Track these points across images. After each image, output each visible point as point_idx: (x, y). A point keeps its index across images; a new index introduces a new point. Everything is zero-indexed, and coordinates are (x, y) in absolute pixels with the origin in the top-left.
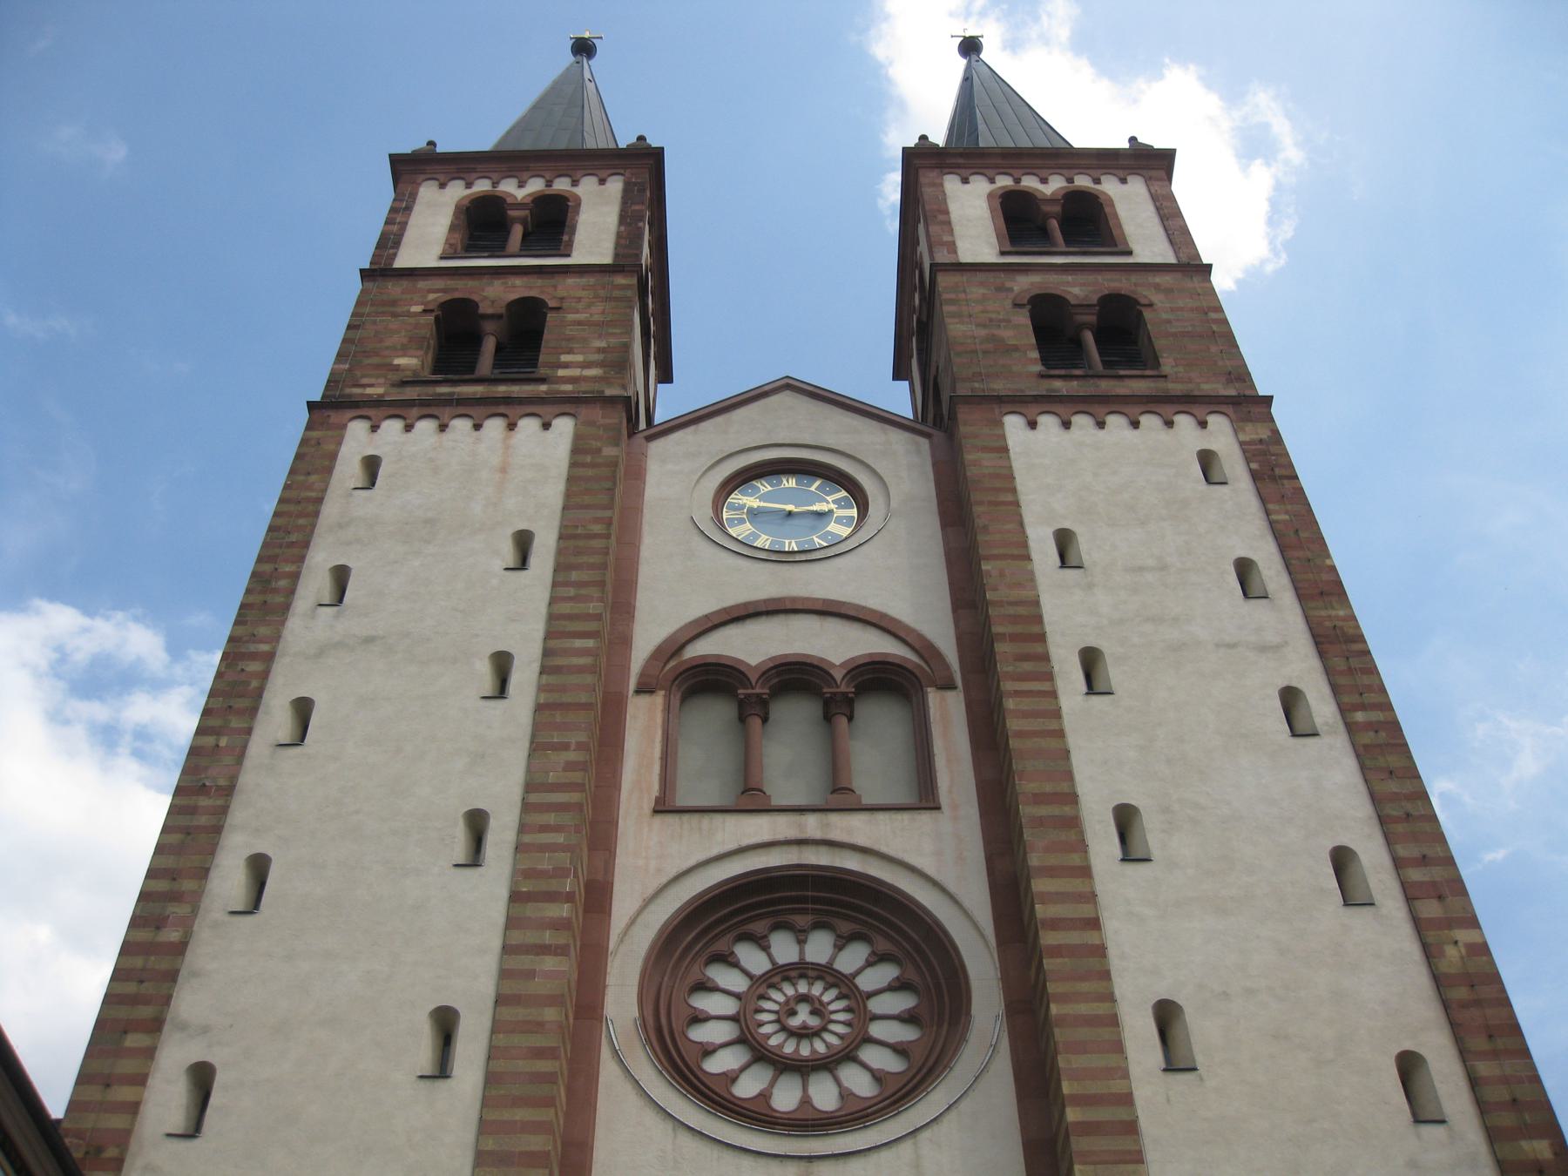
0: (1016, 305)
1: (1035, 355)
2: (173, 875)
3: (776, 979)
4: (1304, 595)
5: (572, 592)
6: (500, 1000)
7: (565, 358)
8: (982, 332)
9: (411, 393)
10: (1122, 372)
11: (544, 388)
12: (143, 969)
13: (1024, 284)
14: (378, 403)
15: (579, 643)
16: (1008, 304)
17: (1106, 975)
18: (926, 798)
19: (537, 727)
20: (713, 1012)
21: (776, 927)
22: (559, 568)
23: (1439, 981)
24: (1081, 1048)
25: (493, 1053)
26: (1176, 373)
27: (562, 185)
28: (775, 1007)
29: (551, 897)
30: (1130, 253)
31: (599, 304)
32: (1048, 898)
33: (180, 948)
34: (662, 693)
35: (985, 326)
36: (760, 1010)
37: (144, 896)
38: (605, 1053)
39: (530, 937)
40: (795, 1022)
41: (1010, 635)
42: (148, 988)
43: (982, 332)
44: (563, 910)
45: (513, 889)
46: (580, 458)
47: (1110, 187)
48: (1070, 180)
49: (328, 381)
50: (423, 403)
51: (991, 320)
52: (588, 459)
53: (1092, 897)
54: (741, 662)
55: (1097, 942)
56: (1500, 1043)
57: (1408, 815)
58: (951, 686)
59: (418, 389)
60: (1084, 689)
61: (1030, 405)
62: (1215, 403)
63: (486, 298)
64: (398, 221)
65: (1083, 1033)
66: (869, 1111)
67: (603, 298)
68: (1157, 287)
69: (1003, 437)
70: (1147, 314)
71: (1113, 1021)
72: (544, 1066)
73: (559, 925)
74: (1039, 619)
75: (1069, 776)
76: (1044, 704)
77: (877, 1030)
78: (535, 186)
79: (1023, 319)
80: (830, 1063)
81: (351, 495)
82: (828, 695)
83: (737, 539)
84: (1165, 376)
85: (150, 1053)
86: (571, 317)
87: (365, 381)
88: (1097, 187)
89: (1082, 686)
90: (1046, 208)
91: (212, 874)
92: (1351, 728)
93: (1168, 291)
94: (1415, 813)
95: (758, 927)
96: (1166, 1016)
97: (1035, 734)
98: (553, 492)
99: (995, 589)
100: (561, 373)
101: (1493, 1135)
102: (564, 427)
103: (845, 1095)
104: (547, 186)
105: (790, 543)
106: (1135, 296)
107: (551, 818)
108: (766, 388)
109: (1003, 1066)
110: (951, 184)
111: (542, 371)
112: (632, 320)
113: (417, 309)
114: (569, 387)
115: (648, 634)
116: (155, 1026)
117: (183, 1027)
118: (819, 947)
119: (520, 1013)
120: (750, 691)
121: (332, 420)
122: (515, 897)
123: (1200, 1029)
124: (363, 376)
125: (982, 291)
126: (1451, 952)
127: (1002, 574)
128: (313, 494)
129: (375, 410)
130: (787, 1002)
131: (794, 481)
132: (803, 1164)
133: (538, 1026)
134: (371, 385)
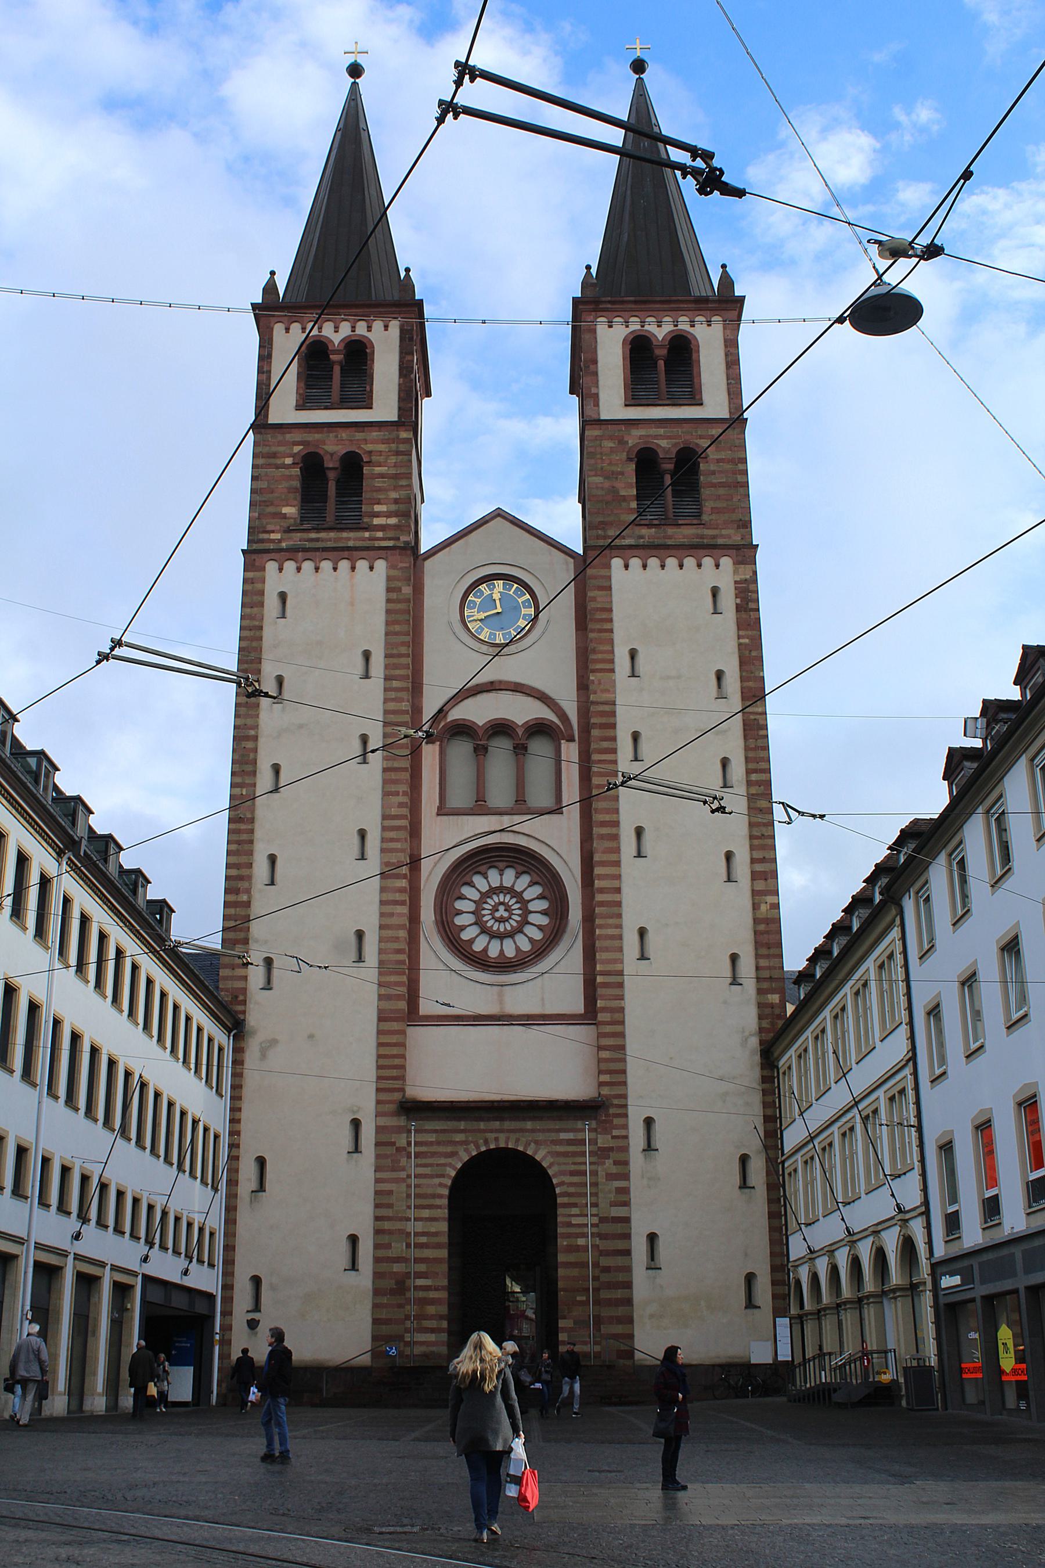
0: (630, 459)
1: (634, 505)
6: (381, 927)
7: (377, 508)
9: (296, 539)
11: (367, 534)
12: (235, 915)
13: (635, 438)
16: (624, 456)
18: (558, 810)
19: (385, 782)
21: (490, 867)
22: (387, 678)
23: (756, 921)
24: (607, 949)
25: (381, 951)
26: (711, 520)
27: (361, 329)
28: (491, 908)
29: (398, 876)
31: (393, 457)
34: (438, 743)
39: (390, 896)
43: (607, 484)
53: (618, 877)
56: (772, 951)
57: (763, 835)
59: (299, 534)
63: (327, 452)
64: (265, 369)
65: (607, 943)
66: (526, 960)
67: (394, 451)
71: (620, 937)
73: (401, 890)
74: (613, 714)
81: (276, 623)
84: (703, 524)
86: (378, 470)
87: (270, 527)
91: (254, 865)
92: (749, 783)
94: (766, 834)
95: (482, 869)
98: (379, 621)
99: (595, 693)
100: (376, 521)
101: (760, 992)
104: (352, 331)
108: (487, 518)
111: (366, 520)
112: (411, 461)
113: (289, 461)
115: (429, 709)
116: (246, 941)
117: (257, 941)
118: (509, 877)
119: (390, 933)
124: (267, 524)
126: (764, 908)
127: (599, 681)
128: (257, 623)
132: (500, 987)
133: (397, 939)
134: (273, 532)
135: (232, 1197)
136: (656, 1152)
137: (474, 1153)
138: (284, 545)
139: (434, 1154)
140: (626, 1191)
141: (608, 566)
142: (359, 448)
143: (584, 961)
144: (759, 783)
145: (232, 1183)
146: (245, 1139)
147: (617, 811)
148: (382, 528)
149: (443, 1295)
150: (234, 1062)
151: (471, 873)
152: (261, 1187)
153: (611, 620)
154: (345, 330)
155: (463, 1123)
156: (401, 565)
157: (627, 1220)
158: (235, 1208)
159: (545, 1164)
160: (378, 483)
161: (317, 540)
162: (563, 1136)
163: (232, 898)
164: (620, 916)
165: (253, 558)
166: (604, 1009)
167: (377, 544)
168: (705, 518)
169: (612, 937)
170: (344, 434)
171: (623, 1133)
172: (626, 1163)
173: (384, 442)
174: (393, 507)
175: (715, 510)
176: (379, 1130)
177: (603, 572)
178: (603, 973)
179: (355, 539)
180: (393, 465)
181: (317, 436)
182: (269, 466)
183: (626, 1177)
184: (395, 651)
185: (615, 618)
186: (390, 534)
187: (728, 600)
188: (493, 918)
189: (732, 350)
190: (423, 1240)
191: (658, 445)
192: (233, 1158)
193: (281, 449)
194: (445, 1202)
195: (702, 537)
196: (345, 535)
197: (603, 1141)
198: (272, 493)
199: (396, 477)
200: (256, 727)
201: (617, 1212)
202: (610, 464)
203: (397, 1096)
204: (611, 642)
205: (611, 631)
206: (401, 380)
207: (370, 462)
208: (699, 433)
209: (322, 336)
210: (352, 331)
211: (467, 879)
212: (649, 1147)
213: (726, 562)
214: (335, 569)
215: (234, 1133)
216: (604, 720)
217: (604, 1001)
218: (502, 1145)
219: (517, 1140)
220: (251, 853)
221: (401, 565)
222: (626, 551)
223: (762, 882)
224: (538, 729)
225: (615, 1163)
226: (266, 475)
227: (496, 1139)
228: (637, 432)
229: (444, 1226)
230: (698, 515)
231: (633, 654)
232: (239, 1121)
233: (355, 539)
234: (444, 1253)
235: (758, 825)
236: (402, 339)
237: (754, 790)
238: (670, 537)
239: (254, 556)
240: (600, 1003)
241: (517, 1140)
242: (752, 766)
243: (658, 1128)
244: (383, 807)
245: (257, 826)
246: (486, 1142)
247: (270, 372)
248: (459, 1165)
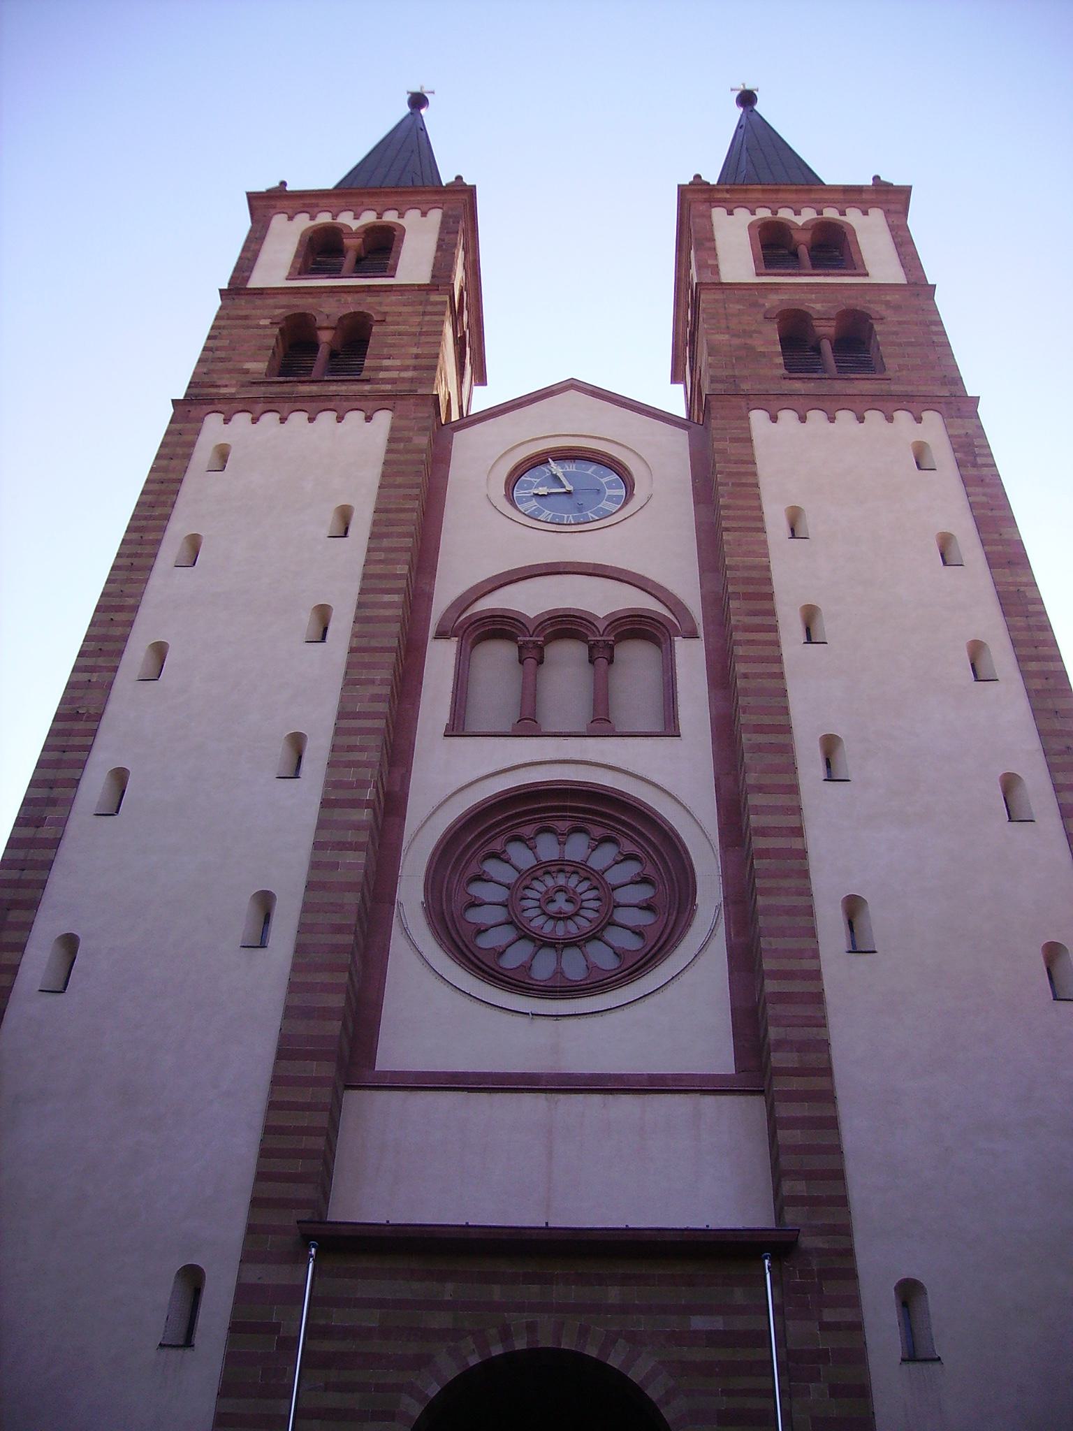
1: (780, 360)
2: (52, 785)
3: (540, 873)
4: (993, 562)
5: (382, 556)
6: (310, 886)
7: (386, 363)
8: (736, 341)
10: (852, 376)
11: (367, 387)
13: (772, 301)
14: (230, 399)
15: (387, 598)
16: (760, 317)
17: (805, 874)
20: (487, 900)
25: (303, 928)
27: (390, 217)
28: (538, 896)
29: (355, 804)
30: (867, 275)
32: (758, 810)
33: (55, 843)
35: (739, 336)
37: (27, 802)
38: (396, 931)
40: (552, 908)
41: (744, 594)
42: (28, 875)
43: (736, 341)
44: (365, 815)
45: (323, 797)
46: (394, 446)
47: (853, 217)
48: (820, 213)
49: (190, 383)
50: (269, 399)
51: (744, 331)
52: (402, 445)
53: (798, 810)
55: (800, 847)
60: (803, 638)
61: (773, 403)
62: (931, 402)
64: (252, 249)
68: (887, 303)
69: (748, 429)
70: (877, 327)
71: (810, 911)
74: (768, 581)
75: (785, 710)
76: (768, 651)
77: (621, 916)
78: (369, 218)
79: (772, 333)
80: (579, 941)
82: (592, 643)
83: (524, 513)
88: (842, 218)
89: (802, 637)
93: (897, 308)
96: (853, 907)
97: (760, 676)
98: (372, 474)
100: (382, 375)
102: (384, 419)
103: (591, 968)
104: (378, 218)
105: (568, 517)
106: (868, 312)
107: (357, 740)
108: (554, 388)
109: (719, 946)
110: (718, 214)
111: (365, 375)
114: (389, 387)
115: (446, 592)
116: (33, 905)
118: (577, 848)
120: (528, 639)
121: (191, 414)
122: (326, 804)
123: (878, 920)
129: (229, 407)
130: (547, 892)
131: (574, 466)
136: (937, 1366)
137: (474, 1360)
143: (730, 973)
151: (504, 837)
155: (450, 1286)
159: (654, 1392)
162: (699, 1323)
165: (187, 409)
166: (781, 1044)
168: (889, 374)
169: (791, 911)
171: (846, 1315)
176: (244, 1292)
180: (417, 324)
187: (942, 454)
188: (544, 913)
193: (259, 312)
198: (234, 350)
206: (439, 254)
207: (384, 321)
208: (868, 298)
209: (336, 223)
210: (378, 218)
211: (497, 846)
217: (781, 1030)
218: (546, 1342)
219: (584, 1332)
225: (836, 1391)
227: (531, 1328)
241: (584, 1332)
243: (936, 1302)
244: (341, 701)
246: (505, 1334)
248: (434, 1390)
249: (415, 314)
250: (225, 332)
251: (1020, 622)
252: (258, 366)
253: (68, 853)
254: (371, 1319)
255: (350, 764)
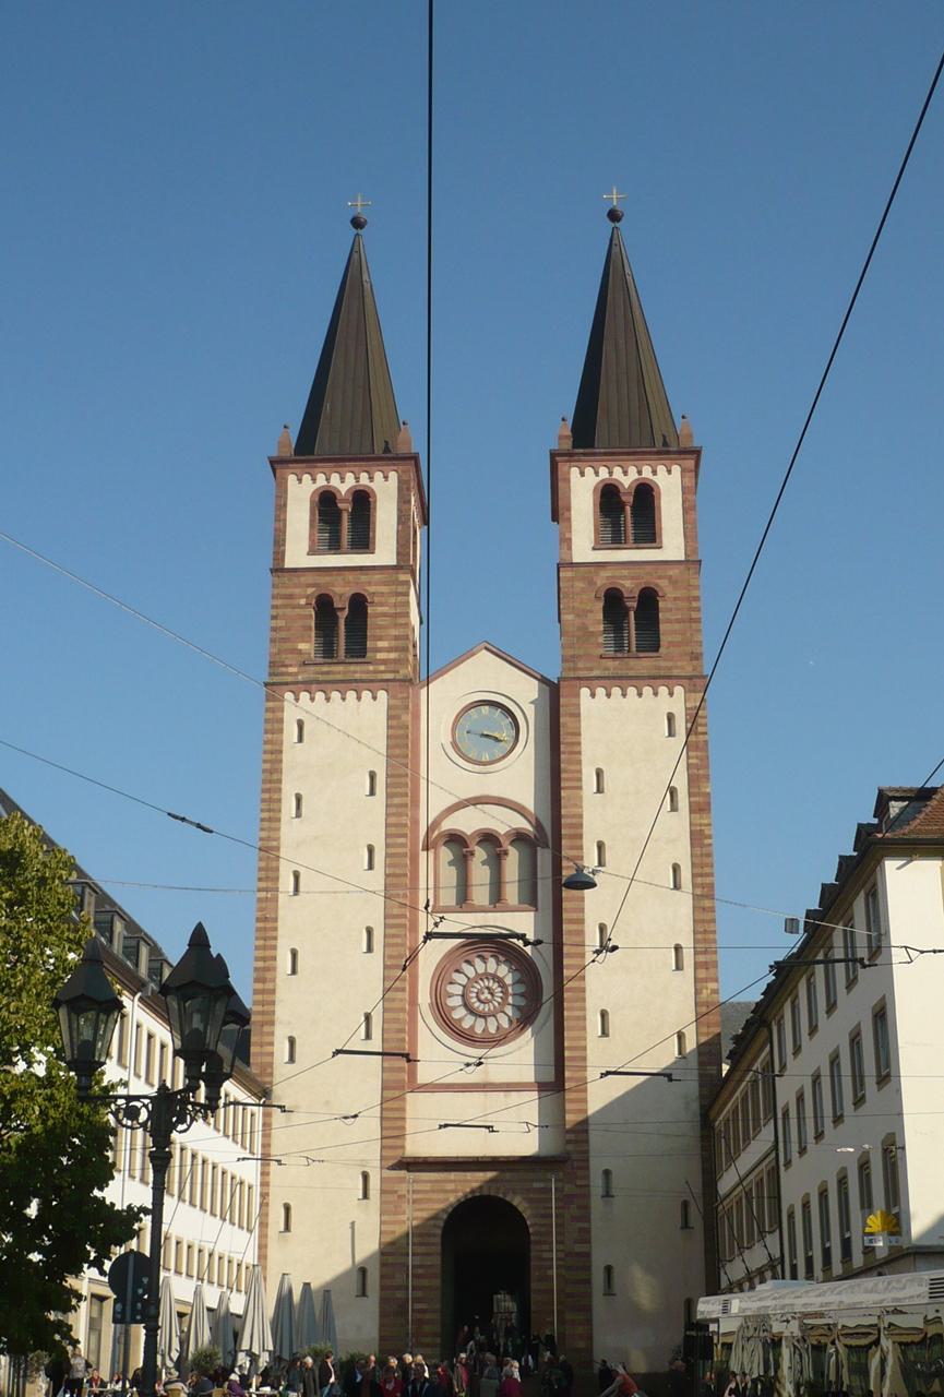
7: (381, 644)
9: (310, 673)
11: (371, 668)
13: (603, 580)
22: (388, 796)
33: (273, 992)
36: (473, 987)
43: (578, 621)
50: (318, 682)
54: (463, 833)
58: (547, 846)
72: (401, 1035)
85: (272, 1034)
86: (380, 609)
87: (287, 662)
90: (624, 498)
93: (673, 582)
100: (380, 656)
111: (368, 654)
113: (303, 602)
116: (272, 1023)
125: (582, 585)
128: (278, 748)
129: (298, 686)
133: (397, 1021)
134: (291, 666)
135: (263, 1236)
138: (300, 678)
139: (429, 1200)
140: (587, 1231)
141: (578, 695)
142: (365, 590)
144: (703, 886)
145: (264, 1225)
146: (272, 1190)
147: (582, 910)
148: (384, 662)
149: (436, 1317)
150: (264, 1125)
152: (287, 1228)
153: (579, 744)
154: (350, 480)
156: (400, 696)
157: (588, 1255)
158: (266, 1246)
160: (381, 621)
161: (328, 673)
162: (536, 1185)
163: (259, 986)
164: (584, 1000)
167: (380, 676)
170: (350, 577)
172: (586, 1208)
173: (384, 584)
174: (393, 643)
175: (671, 644)
176: (383, 1180)
177: (573, 700)
178: (570, 1048)
179: (362, 672)
181: (328, 579)
182: (285, 606)
183: (586, 1218)
184: (396, 772)
185: (583, 742)
186: (392, 667)
187: (681, 726)
189: (689, 497)
190: (420, 1271)
191: (624, 587)
192: (264, 1205)
193: (297, 591)
194: (438, 1240)
195: (659, 668)
196: (352, 668)
197: (568, 1189)
199: (396, 615)
200: (278, 839)
201: (579, 1248)
202: (581, 602)
203: (398, 1153)
204: (579, 762)
205: (580, 753)
212: (607, 1194)
213: (679, 690)
214: (344, 699)
215: (265, 1184)
216: (572, 831)
220: (274, 948)
221: (400, 696)
222: (591, 681)
223: (704, 970)
224: (519, 837)
225: (579, 1207)
226: (284, 615)
228: (605, 574)
229: (437, 1260)
230: (656, 648)
231: (599, 773)
232: (268, 1174)
233: (362, 672)
234: (437, 1282)
235: (703, 921)
236: (400, 490)
237: (699, 892)
238: (631, 669)
239: (275, 688)
240: (567, 1074)
241: (498, 1189)
242: (696, 871)
243: (614, 1176)
245: (280, 923)
247: (285, 520)
249: (391, 594)
250: (281, 611)
251: (698, 851)
252: (308, 646)
253: (280, 995)
254: (427, 1187)
255: (393, 945)
